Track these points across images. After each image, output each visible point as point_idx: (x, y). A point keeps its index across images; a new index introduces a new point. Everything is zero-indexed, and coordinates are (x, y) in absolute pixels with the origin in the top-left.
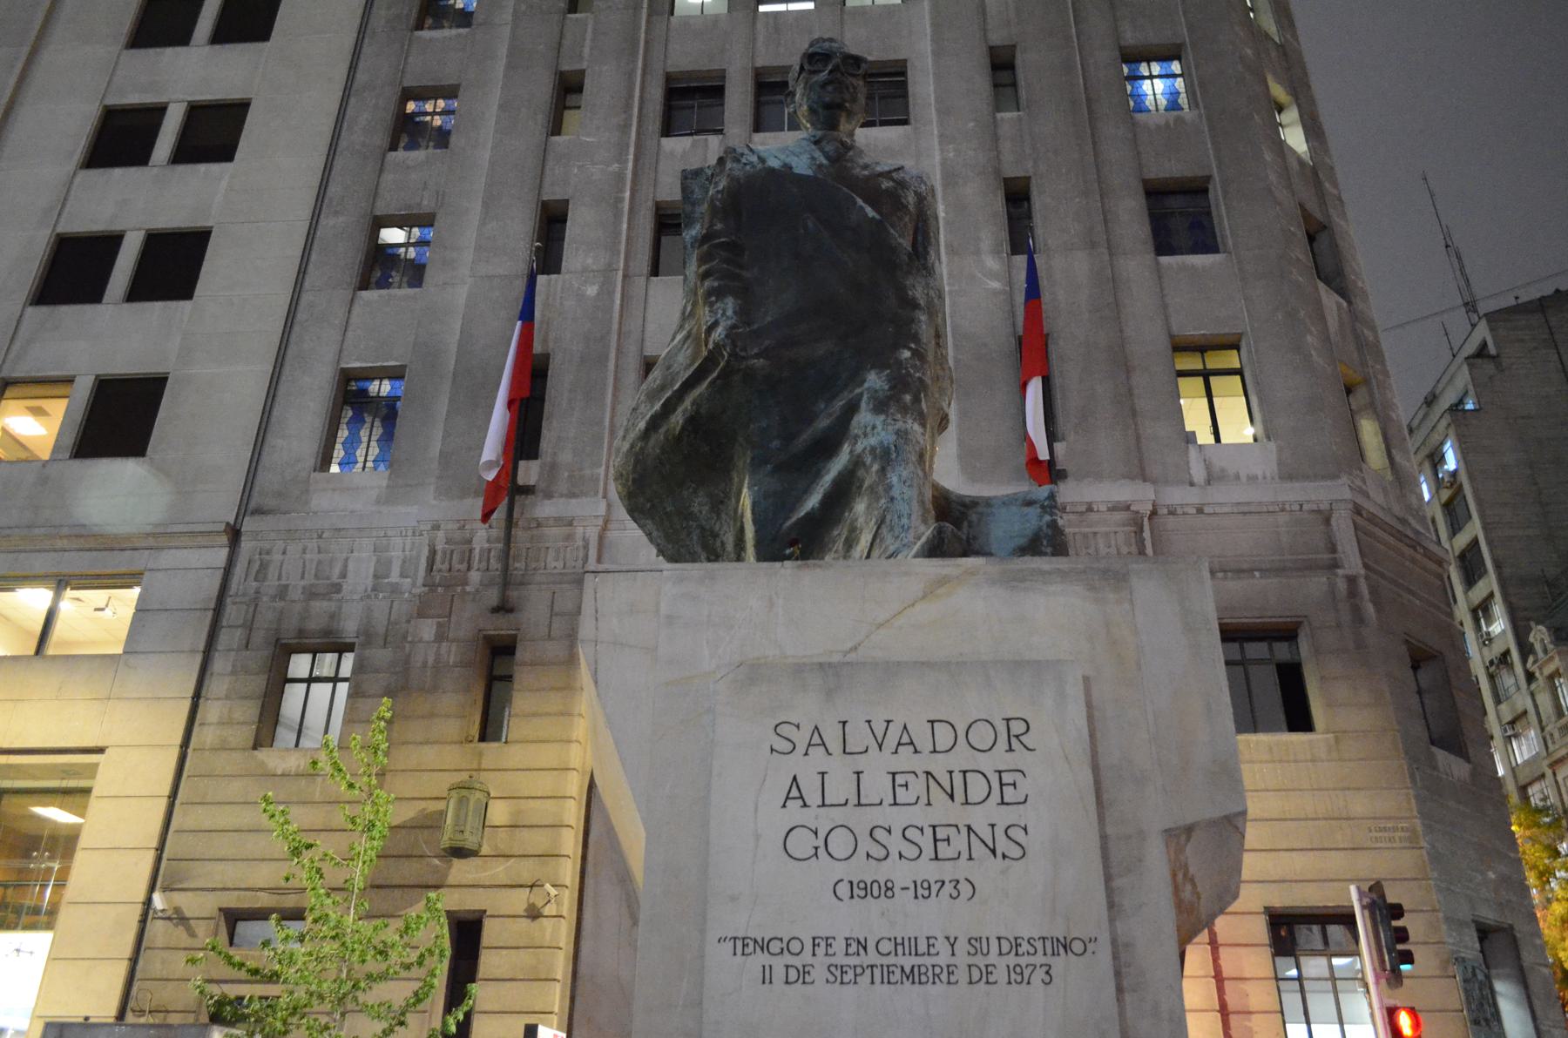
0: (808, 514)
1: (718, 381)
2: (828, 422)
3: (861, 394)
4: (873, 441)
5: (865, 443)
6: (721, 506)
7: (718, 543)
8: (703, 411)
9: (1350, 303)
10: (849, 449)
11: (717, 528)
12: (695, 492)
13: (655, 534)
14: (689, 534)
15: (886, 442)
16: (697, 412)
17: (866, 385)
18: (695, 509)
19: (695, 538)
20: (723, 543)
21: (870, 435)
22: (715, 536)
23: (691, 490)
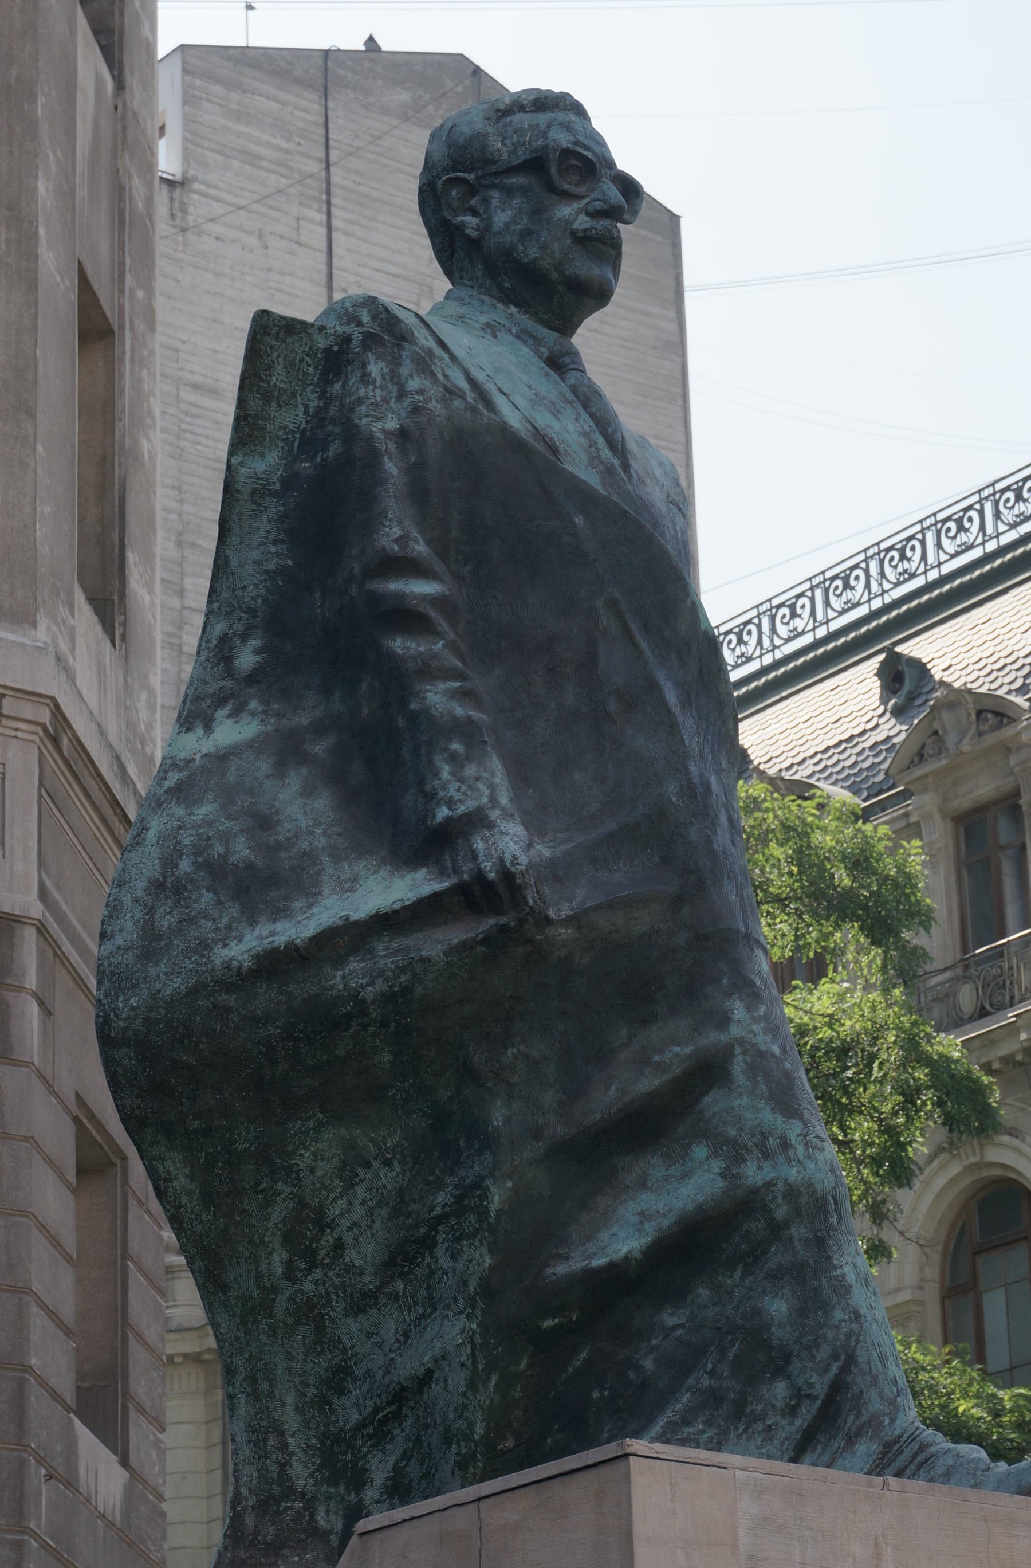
0: (612, 1266)
1: (480, 949)
2: (657, 1082)
3: (727, 1053)
4: (793, 1174)
5: (768, 1173)
6: (360, 1171)
7: (328, 1239)
8: (418, 990)
9: (120, 86)
10: (717, 1165)
11: (334, 1211)
12: (320, 1126)
13: (180, 1182)
14: (268, 1203)
15: (819, 1187)
16: (407, 990)
17: (735, 1031)
18: (304, 1160)
19: (276, 1217)
20: (339, 1246)
21: (781, 1159)
22: (322, 1223)
23: (311, 1124)
